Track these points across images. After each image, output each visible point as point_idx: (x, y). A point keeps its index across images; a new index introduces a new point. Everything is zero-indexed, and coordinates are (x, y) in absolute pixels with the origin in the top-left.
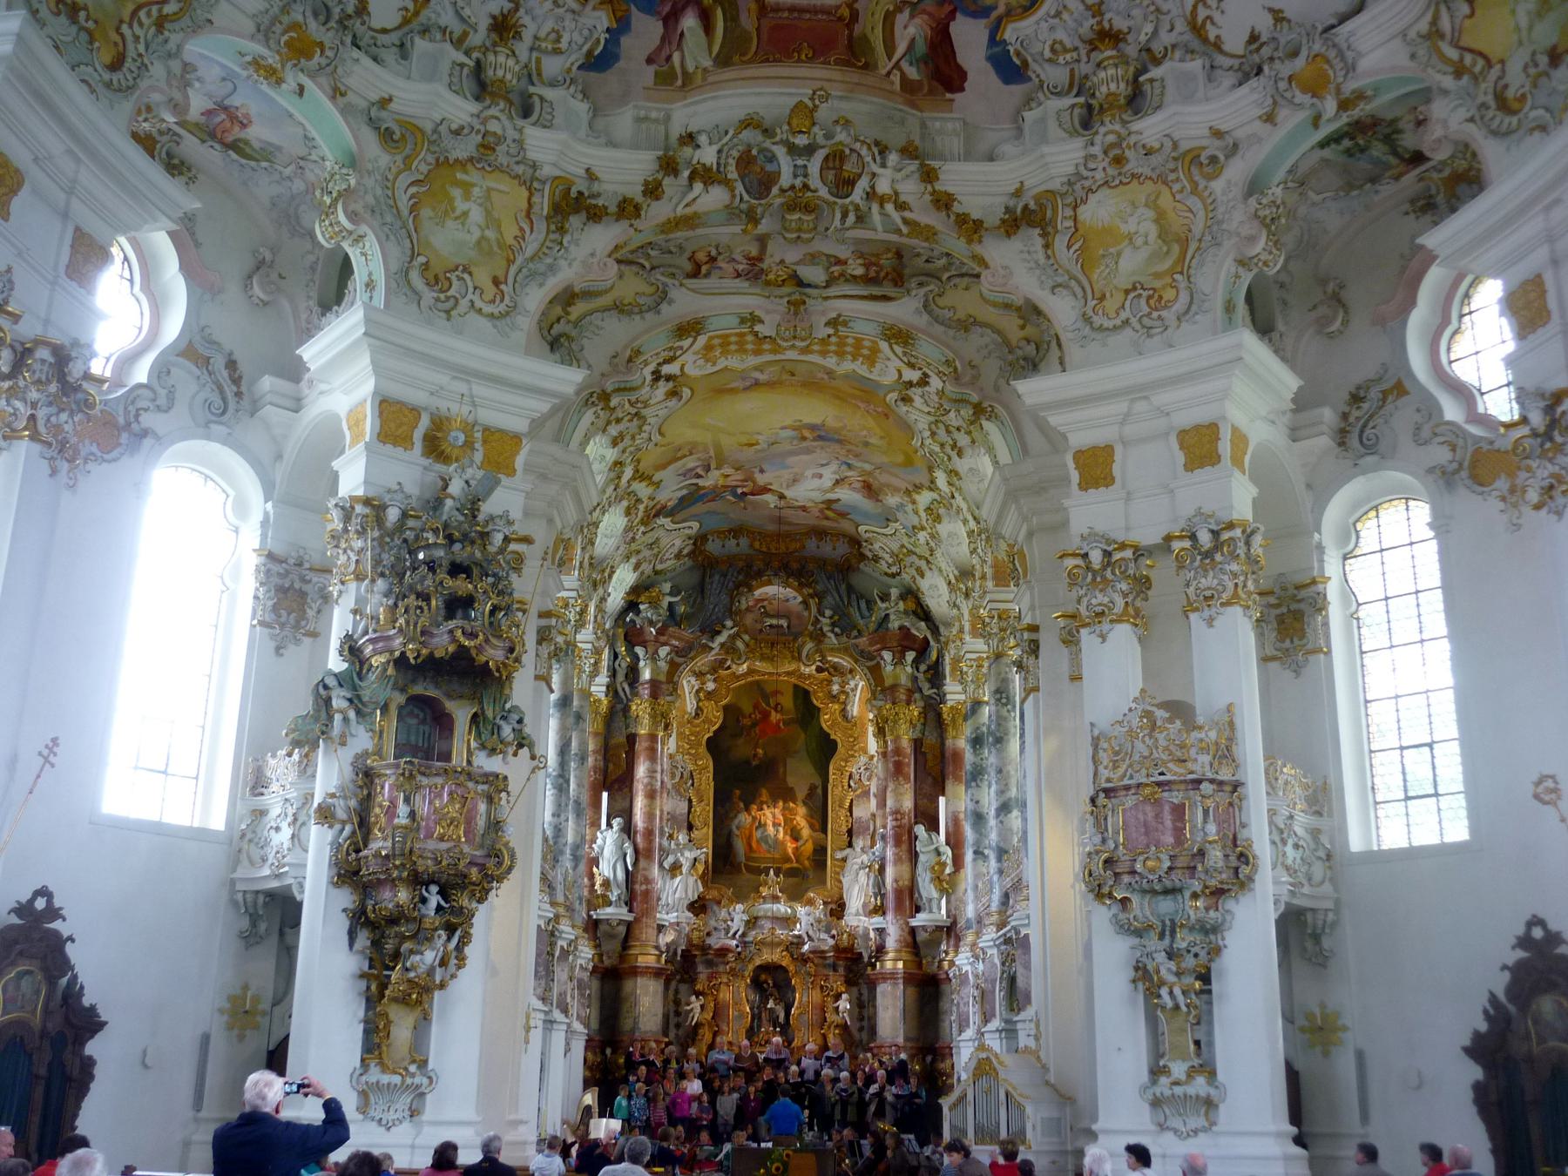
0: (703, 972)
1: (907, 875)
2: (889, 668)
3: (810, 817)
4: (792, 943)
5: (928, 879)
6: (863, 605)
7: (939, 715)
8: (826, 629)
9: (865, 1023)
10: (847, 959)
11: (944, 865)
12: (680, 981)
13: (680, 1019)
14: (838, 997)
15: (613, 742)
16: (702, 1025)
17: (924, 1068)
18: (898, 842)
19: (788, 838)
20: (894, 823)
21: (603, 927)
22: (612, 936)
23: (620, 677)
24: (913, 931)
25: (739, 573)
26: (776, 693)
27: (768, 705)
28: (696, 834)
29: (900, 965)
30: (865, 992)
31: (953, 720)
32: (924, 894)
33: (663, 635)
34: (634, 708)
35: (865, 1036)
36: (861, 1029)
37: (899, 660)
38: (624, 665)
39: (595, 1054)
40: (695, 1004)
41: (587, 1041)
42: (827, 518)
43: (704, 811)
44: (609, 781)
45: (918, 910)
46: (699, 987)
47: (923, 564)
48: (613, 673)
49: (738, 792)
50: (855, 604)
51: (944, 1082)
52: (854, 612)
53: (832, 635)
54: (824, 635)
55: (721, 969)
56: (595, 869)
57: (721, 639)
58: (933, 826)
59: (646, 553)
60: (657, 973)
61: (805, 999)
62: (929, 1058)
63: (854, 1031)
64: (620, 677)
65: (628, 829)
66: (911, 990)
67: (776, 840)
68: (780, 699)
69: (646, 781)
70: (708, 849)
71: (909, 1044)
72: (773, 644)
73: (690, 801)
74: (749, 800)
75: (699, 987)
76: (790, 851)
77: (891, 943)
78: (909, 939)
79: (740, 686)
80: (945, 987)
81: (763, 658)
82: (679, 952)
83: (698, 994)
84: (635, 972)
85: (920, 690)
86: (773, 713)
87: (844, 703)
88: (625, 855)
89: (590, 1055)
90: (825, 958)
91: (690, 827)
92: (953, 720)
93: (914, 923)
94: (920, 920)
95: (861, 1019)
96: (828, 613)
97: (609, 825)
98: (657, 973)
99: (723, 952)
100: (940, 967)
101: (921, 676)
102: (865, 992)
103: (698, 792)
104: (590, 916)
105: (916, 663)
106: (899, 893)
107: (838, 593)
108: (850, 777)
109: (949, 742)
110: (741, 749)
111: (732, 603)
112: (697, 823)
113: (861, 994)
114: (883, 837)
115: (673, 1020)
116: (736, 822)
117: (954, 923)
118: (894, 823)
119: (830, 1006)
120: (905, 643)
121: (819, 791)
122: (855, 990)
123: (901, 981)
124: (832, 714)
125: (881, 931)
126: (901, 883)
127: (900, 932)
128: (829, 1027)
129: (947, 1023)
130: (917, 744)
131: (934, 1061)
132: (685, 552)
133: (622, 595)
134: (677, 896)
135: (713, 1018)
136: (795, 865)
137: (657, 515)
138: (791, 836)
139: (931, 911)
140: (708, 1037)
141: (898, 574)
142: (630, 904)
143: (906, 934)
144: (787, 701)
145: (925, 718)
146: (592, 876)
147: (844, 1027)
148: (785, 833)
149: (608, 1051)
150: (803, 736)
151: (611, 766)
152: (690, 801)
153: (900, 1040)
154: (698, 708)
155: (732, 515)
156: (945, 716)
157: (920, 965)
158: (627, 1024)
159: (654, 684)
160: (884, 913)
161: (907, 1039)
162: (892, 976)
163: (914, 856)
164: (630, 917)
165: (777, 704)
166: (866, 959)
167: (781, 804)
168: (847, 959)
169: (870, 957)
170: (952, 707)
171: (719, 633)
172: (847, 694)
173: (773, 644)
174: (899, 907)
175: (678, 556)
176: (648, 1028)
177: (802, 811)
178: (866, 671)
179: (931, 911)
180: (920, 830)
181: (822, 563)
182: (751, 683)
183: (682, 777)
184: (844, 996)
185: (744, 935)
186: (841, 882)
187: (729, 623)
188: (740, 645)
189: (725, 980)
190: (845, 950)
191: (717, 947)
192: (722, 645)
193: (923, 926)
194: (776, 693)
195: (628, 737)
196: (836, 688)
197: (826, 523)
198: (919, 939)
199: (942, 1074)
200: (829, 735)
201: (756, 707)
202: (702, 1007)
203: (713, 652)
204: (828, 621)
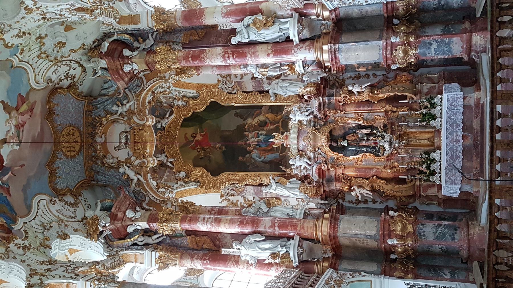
0: (336, 186)
1: (265, 46)
2: (135, 66)
3: (253, 116)
4: (314, 126)
5: (267, 32)
6: (106, 86)
7: (166, 32)
8: (125, 110)
9: (371, 73)
10: (324, 88)
11: (255, 23)
12: (344, 200)
13: (369, 200)
14: (351, 92)
15: (190, 245)
16: (372, 187)
17: (403, 24)
18: (243, 55)
19: (265, 128)
20: (231, 58)
21: (304, 257)
22: (311, 250)
23: (149, 240)
24: (302, 41)
25: (96, 164)
26: (186, 138)
27: (192, 141)
28: (264, 182)
29: (325, 47)
30: (348, 75)
31: (164, 21)
32: (276, 35)
33: (117, 215)
34: (167, 232)
35: (379, 73)
36: (375, 75)
37: (128, 60)
38: (141, 238)
39: (395, 269)
40: (357, 192)
41: (385, 275)
42: (32, 110)
43: (253, 178)
44: (214, 248)
45: (288, 40)
46: (346, 189)
47: (49, 44)
48: (147, 245)
49: (240, 158)
50: (106, 91)
51: (414, 7)
52: (111, 91)
53: (128, 105)
54: (129, 109)
55: (333, 174)
56: (266, 262)
57: (132, 174)
58: (233, 32)
59: (52, 234)
60: (334, 220)
61: (353, 116)
62: (395, 21)
63: (375, 81)
64: (149, 240)
65: (240, 237)
66: (344, 38)
67: (266, 135)
68: (189, 136)
69: (209, 226)
70: (271, 174)
71: (385, 35)
72: (135, 142)
73: (246, 185)
74: (245, 152)
75: (346, 189)
76: (272, 127)
77: (310, 56)
78: (308, 43)
79: (183, 158)
80: (342, 13)
81: (145, 148)
82: (323, 202)
83: (350, 190)
84: (333, 237)
85: (152, 45)
86: (195, 139)
87: (189, 98)
88: (255, 241)
89: (397, 274)
90: (324, 103)
91: (261, 185)
92: (164, 21)
93: (296, 41)
94: (294, 37)
95: (368, 76)
96: (115, 108)
97: (239, 249)
98: (334, 220)
99: (321, 173)
100: (327, 19)
101: (143, 46)
102: (348, 75)
103: (240, 181)
104: (297, 267)
105: (132, 49)
106: (276, 53)
107: (104, 102)
108: (230, 93)
109: (180, 24)
110: (217, 157)
111: (113, 167)
112: (258, 181)
113: (350, 77)
114: (246, 66)
115: (371, 205)
116: (257, 159)
117: (296, 10)
118: (231, 58)
119: (358, 98)
120: (116, 55)
121: (238, 111)
122: (347, 82)
123: (337, 46)
124: (196, 105)
125: (305, 65)
126: (270, 52)
127: (303, 50)
128: (372, 98)
129: (369, 9)
130: (185, 46)
131: (397, 18)
132: (72, 200)
133: (93, 242)
134: (298, 193)
135: (367, 179)
136: (280, 123)
137: (9, 231)
138: (264, 127)
139: (288, 29)
140: (381, 182)
141: (77, 62)
142: (289, 238)
143: (305, 45)
144: (190, 131)
145: (169, 42)
146: (270, 265)
147: (372, 88)
148: (263, 130)
149: (393, 257)
150: (208, 121)
151: (205, 246)
152: (246, 185)
153: (381, 43)
154: (194, 182)
155: (31, 174)
156: (162, 27)
157: (327, 34)
158: (372, 244)
159: (150, 221)
160: (293, 63)
161: (380, 38)
162: (333, 53)
163: (252, 44)
164: (297, 238)
165: (192, 136)
166: (325, 75)
167: (246, 133)
168: (324, 88)
169: (325, 72)
170: (156, 22)
171: (128, 176)
172: (184, 96)
173: (135, 142)
174: (286, 52)
175: (75, 205)
176: (375, 229)
177: (249, 121)
178: (149, 83)
179: (288, 29)
180: (234, 41)
181: (88, 112)
182: (180, 151)
183: (233, 190)
184: (350, 88)
185: (309, 159)
186: (290, 96)
187: (121, 170)
188: (137, 162)
189: (341, 171)
190: (318, 89)
191: (317, 177)
192: (137, 173)
193: (300, 32)
194: (186, 138)
195: (188, 235)
196: (180, 103)
197: (38, 110)
198: (308, 36)
199: (407, 10)
200: (207, 106)
201: (194, 149)
202: (360, 187)
203: (141, 179)
204: (120, 108)
